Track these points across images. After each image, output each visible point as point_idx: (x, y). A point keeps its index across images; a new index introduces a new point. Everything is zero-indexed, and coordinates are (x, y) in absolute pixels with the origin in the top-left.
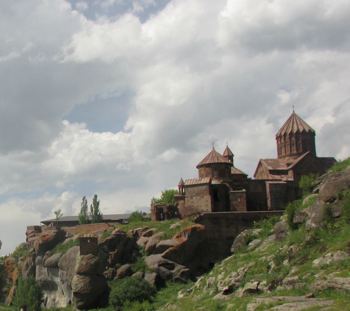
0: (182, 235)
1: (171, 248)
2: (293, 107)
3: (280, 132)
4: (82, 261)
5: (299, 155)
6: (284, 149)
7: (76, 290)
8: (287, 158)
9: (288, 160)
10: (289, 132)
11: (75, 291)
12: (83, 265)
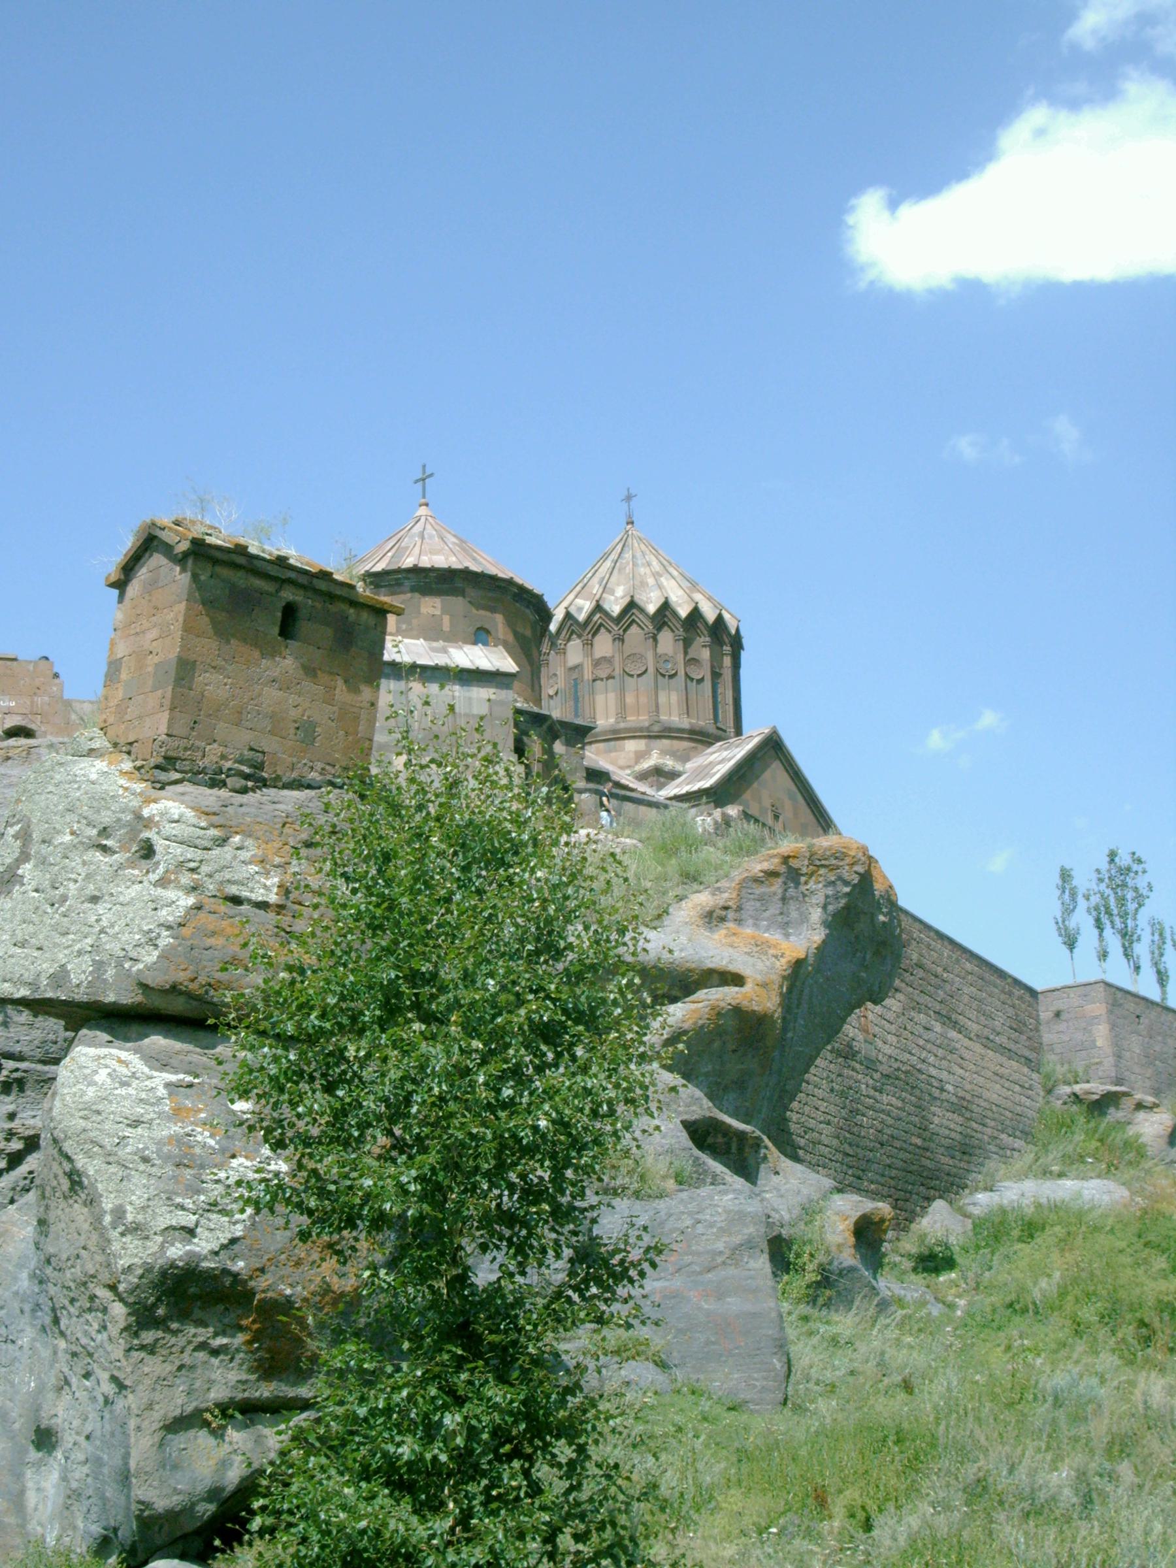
0: (750, 906)
1: (725, 995)
2: (629, 498)
3: (587, 606)
4: (227, 852)
5: (703, 738)
6: (612, 696)
7: (191, 1232)
8: (631, 746)
9: (640, 756)
10: (651, 609)
11: (176, 1251)
12: (236, 900)
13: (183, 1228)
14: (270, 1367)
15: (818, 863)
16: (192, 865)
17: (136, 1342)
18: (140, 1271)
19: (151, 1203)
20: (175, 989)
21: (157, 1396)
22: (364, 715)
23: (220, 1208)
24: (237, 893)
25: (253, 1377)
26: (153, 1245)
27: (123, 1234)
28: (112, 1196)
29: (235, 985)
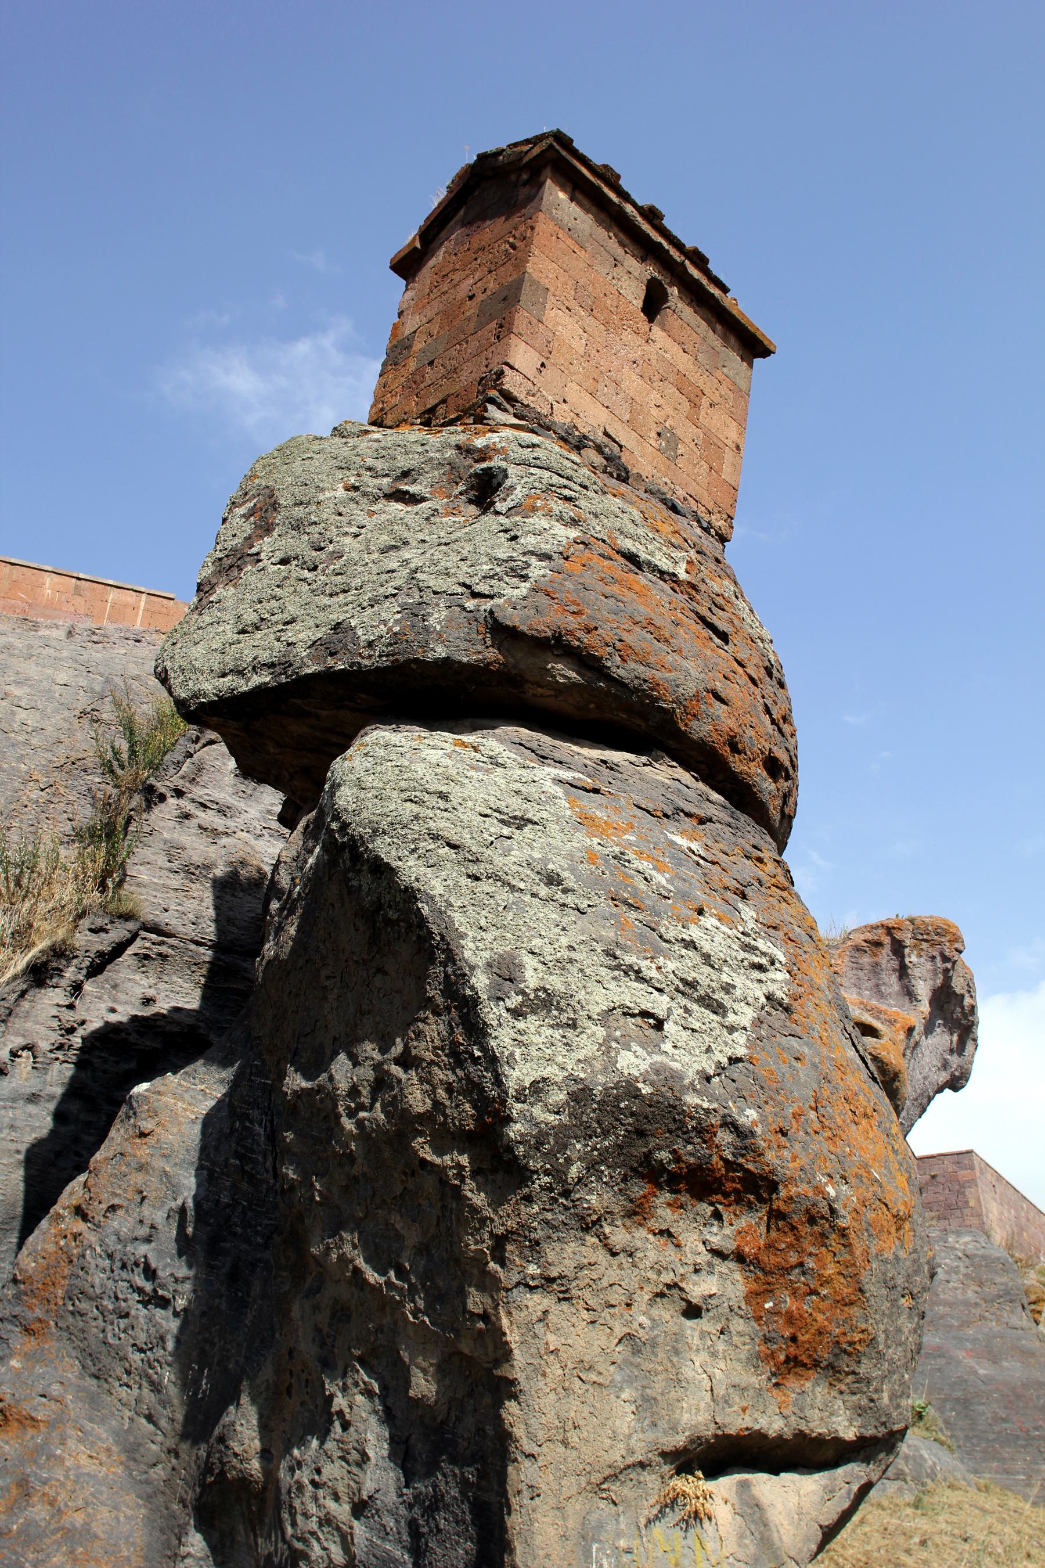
11: (633, 1062)
13: (645, 1014)
14: (788, 1360)
15: (920, 937)
16: (567, 492)
17: (532, 1269)
18: (558, 1097)
19: (573, 955)
20: (557, 645)
21: (573, 1409)
22: (729, 455)
23: (702, 993)
24: (634, 550)
25: (754, 1380)
26: (589, 1041)
27: (517, 1013)
28: (489, 936)
29: (652, 660)
